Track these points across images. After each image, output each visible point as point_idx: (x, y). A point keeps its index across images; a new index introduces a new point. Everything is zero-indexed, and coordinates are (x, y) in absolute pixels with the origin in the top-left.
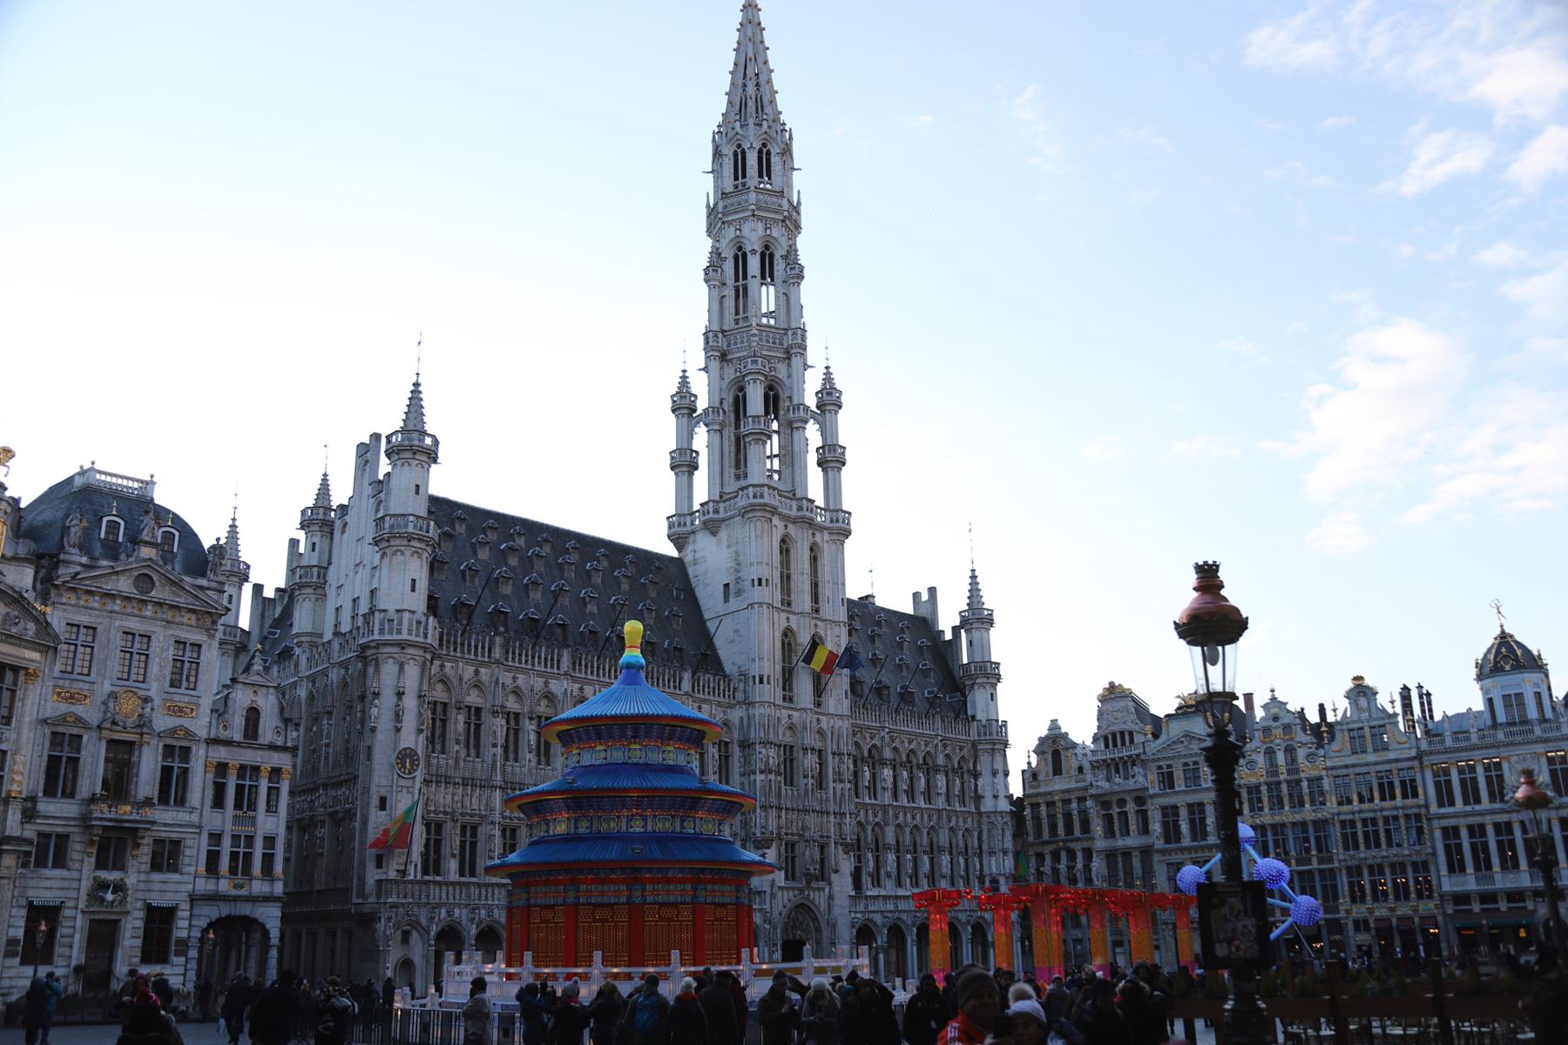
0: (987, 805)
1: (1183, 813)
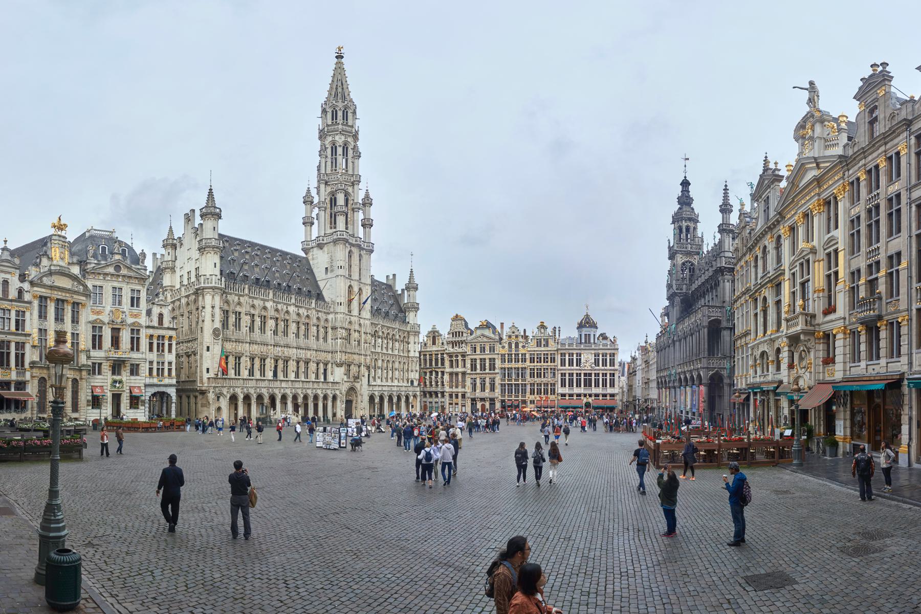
0: (412, 354)
1: (478, 361)
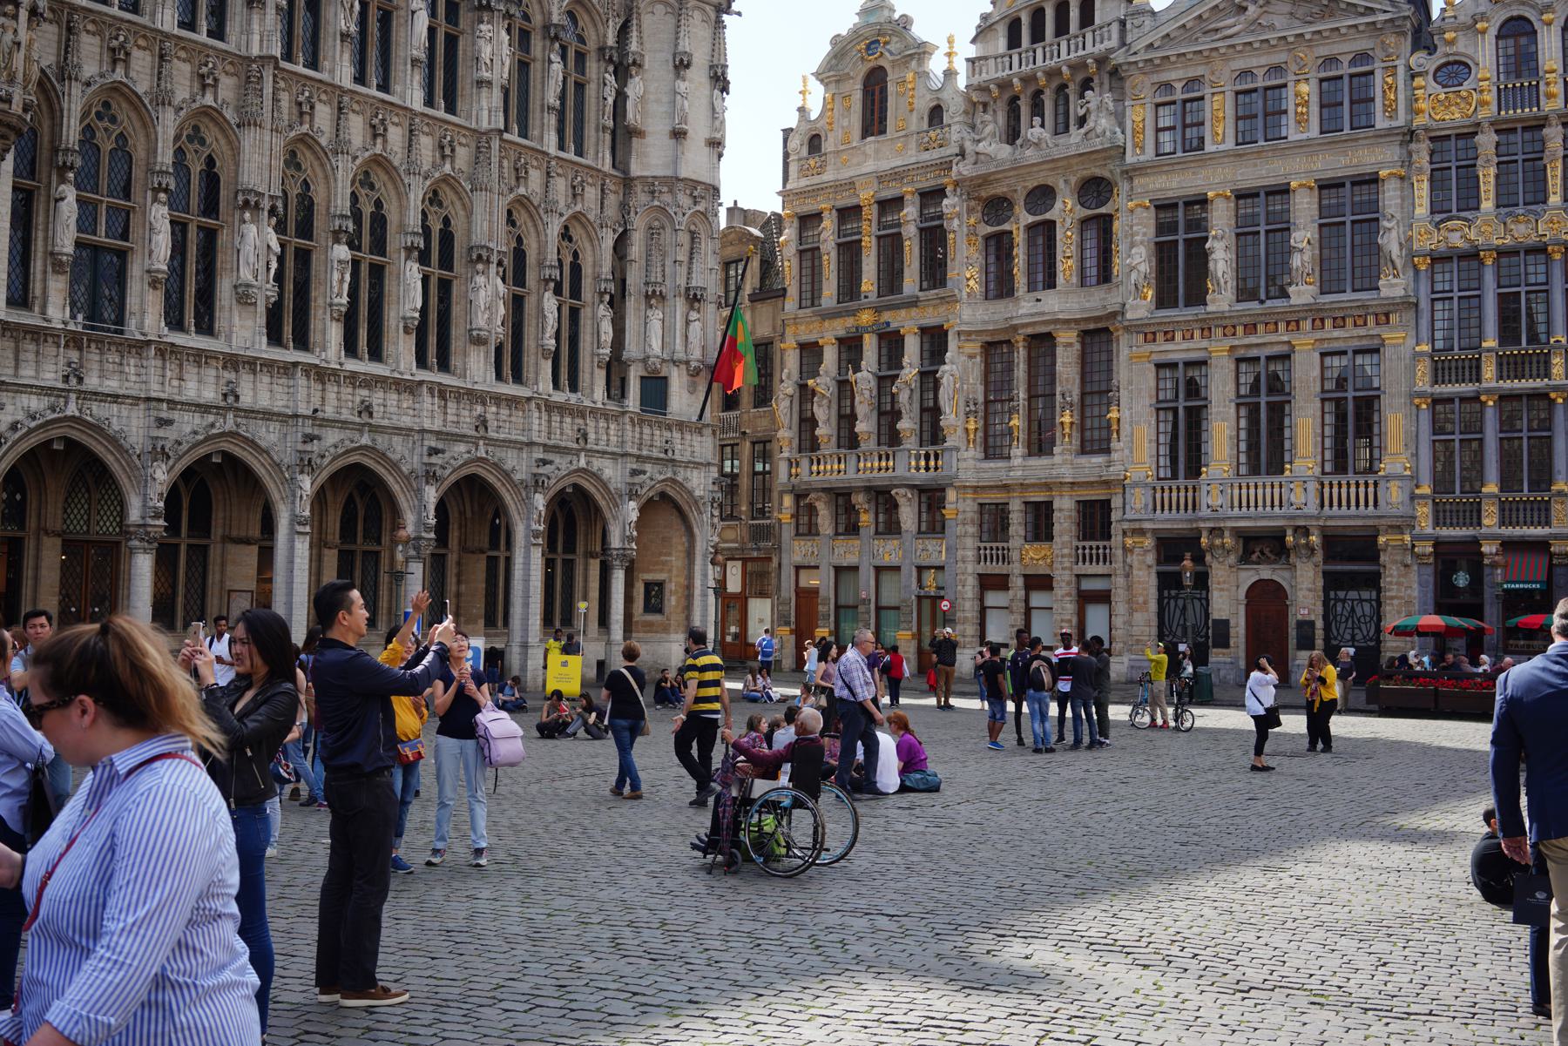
0: (650, 159)
1: (1221, 220)
